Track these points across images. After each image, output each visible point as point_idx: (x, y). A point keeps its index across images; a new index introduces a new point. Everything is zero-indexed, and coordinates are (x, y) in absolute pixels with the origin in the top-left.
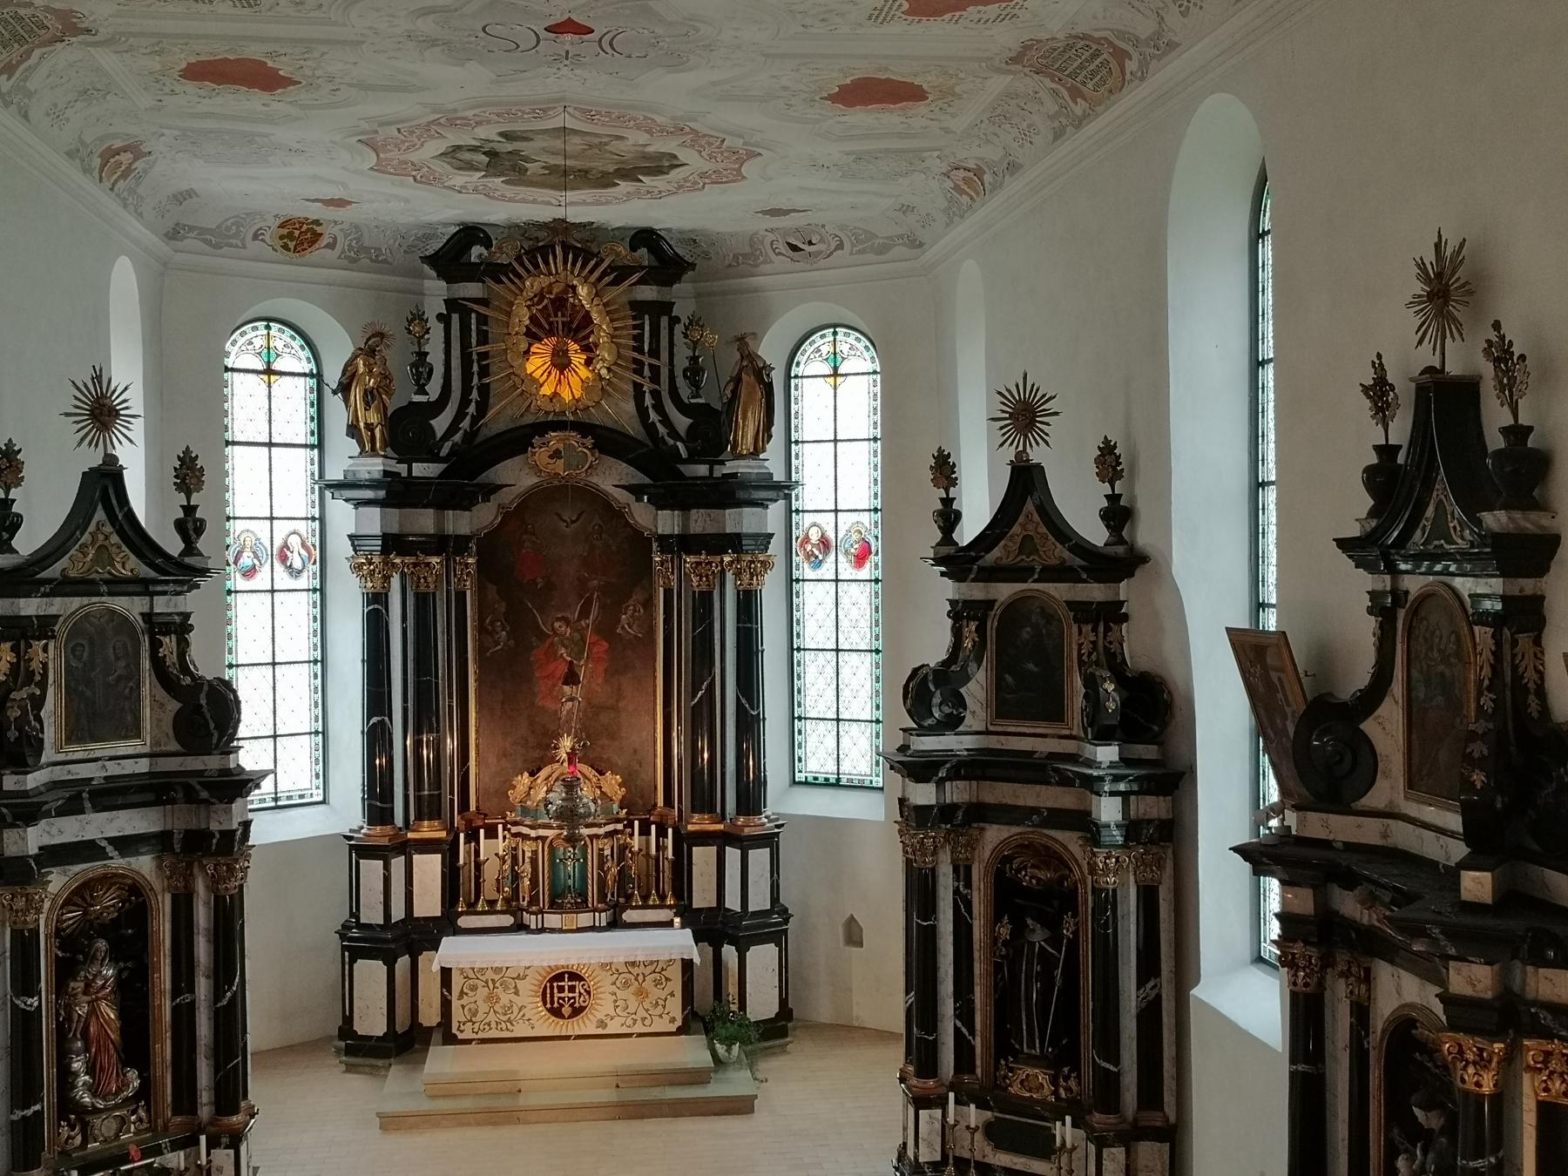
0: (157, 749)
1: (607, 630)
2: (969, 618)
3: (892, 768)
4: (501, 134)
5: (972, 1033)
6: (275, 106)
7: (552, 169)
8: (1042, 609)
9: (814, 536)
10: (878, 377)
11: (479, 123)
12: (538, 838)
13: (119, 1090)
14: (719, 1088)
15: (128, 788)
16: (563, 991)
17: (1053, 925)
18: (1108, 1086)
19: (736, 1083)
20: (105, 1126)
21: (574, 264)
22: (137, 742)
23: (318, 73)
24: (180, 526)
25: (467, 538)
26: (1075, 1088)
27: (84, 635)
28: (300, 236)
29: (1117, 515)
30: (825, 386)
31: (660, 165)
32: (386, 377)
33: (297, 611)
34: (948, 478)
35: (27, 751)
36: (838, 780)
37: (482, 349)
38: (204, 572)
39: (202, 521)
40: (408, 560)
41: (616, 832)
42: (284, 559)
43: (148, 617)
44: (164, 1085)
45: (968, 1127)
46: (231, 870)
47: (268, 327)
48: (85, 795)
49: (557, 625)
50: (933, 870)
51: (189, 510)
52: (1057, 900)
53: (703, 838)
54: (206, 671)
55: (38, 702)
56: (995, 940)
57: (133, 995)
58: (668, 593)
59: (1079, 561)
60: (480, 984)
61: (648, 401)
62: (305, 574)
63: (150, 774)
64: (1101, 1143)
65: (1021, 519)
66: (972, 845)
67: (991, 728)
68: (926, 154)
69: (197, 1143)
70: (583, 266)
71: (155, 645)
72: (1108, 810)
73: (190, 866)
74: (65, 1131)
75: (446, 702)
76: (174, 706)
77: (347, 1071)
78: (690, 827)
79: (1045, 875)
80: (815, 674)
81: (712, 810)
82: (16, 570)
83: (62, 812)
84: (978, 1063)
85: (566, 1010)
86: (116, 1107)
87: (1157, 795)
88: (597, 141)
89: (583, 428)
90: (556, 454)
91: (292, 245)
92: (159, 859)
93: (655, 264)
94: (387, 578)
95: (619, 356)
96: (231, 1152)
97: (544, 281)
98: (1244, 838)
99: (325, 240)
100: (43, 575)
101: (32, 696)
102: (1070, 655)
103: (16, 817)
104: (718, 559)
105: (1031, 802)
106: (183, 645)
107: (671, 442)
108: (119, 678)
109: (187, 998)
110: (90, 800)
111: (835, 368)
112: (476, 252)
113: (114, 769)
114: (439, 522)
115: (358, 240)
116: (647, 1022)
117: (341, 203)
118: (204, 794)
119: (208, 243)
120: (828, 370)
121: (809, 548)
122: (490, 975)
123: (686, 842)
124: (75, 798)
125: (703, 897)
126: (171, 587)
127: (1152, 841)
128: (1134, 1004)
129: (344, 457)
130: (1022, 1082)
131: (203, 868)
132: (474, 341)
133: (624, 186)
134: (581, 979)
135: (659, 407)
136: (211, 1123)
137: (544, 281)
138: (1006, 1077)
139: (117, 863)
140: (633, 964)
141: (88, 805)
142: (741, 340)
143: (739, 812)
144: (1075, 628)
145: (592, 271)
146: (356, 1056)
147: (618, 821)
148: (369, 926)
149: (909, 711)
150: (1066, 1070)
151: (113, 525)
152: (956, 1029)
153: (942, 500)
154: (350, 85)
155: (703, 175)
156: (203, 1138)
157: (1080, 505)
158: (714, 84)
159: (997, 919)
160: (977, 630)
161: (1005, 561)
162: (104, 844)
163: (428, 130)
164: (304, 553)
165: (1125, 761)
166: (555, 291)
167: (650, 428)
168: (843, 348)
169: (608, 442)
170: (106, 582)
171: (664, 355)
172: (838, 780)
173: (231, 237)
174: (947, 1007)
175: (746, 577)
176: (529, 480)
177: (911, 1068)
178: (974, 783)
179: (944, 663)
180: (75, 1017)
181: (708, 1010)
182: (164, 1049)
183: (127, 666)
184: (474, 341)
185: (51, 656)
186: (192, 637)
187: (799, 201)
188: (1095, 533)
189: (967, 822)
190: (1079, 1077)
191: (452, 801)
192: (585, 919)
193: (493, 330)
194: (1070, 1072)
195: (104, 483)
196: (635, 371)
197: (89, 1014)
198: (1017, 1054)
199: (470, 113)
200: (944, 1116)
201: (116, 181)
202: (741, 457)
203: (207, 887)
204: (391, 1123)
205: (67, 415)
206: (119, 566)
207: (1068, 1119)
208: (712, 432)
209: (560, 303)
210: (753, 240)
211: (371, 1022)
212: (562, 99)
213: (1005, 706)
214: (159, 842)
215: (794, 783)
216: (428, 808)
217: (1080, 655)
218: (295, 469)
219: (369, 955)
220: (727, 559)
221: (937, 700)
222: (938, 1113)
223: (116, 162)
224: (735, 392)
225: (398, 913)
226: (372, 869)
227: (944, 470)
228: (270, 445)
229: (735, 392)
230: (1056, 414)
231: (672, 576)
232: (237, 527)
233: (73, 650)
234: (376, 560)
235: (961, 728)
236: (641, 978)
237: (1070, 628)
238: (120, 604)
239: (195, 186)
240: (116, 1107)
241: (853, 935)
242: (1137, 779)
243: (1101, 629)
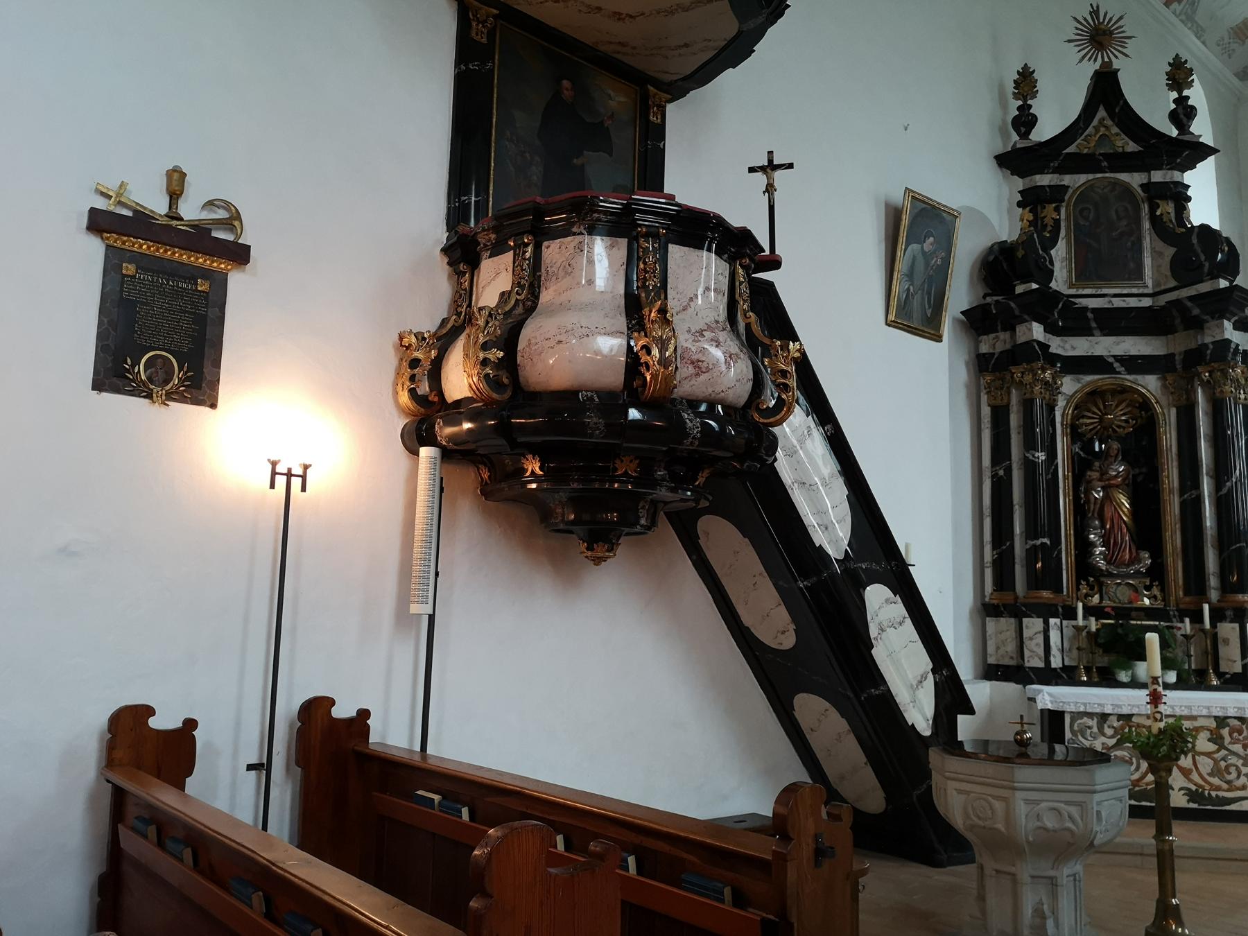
0: (1157, 290)
13: (1132, 562)
24: (1174, 117)
39: (1193, 108)
46: (1225, 374)
51: (1182, 101)
74: (1084, 590)
76: (1170, 251)
92: (1164, 379)
96: (1236, 626)
110: (1095, 319)
113: (1118, 303)
139: (1129, 379)
151: (1113, 120)
162: (1111, 360)
180: (1092, 500)
182: (1173, 538)
185: (1063, 216)
195: (1105, 89)
205: (1069, 41)
233: (1081, 211)
238: (1124, 177)
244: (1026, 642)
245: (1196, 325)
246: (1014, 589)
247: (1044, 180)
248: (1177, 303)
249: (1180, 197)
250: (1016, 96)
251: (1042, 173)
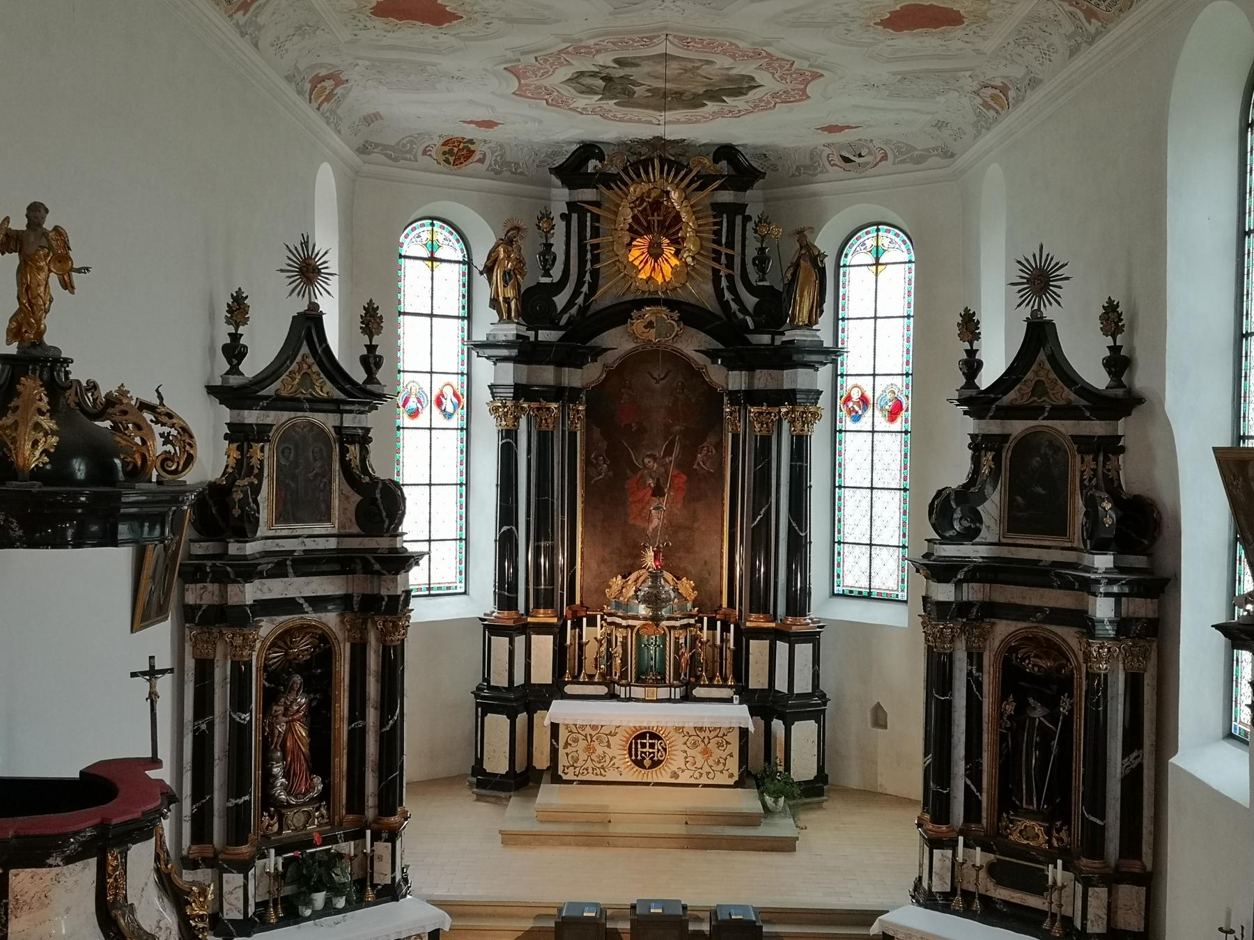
0: (343, 531)
1: (686, 465)
2: (987, 449)
3: (918, 571)
4: (616, 61)
5: (980, 789)
6: (443, 38)
7: (655, 91)
8: (1050, 442)
9: (856, 395)
10: (913, 266)
11: (598, 51)
12: (627, 627)
13: (308, 791)
14: (766, 830)
15: (321, 559)
16: (645, 747)
17: (1051, 704)
18: (1094, 841)
19: (782, 827)
20: (295, 818)
21: (668, 174)
22: (327, 525)
23: (476, 8)
24: (364, 361)
25: (579, 390)
26: (1065, 838)
27: (292, 441)
28: (458, 153)
29: (1118, 363)
30: (868, 273)
31: (740, 86)
32: (520, 261)
33: (449, 444)
34: (973, 333)
35: (247, 526)
36: (870, 593)
37: (595, 241)
38: (381, 397)
39: (381, 357)
40: (534, 405)
41: (689, 625)
42: (439, 403)
43: (339, 429)
44: (340, 791)
45: (974, 866)
46: (395, 626)
47: (432, 225)
48: (289, 563)
49: (646, 460)
50: (951, 656)
51: (371, 348)
52: (1056, 685)
53: (758, 633)
54: (380, 474)
55: (256, 490)
56: (1002, 715)
57: (320, 719)
59: (1083, 402)
61: (724, 283)
62: (455, 416)
63: (336, 550)
64: (1087, 883)
65: (1034, 367)
66: (984, 636)
67: (1003, 540)
68: (960, 74)
69: (364, 837)
70: (675, 176)
71: (344, 451)
72: (1103, 609)
73: (365, 622)
74: (266, 819)
75: (560, 518)
76: (357, 498)
77: (478, 800)
78: (748, 624)
79: (1046, 664)
80: (853, 508)
81: (766, 611)
82: (242, 387)
83: (271, 575)
84: (984, 814)
85: (647, 762)
86: (304, 804)
87: (1145, 597)
88: (690, 65)
89: (672, 304)
90: (650, 325)
91: (451, 159)
92: (342, 615)
94: (517, 419)
95: (702, 247)
97: (645, 187)
98: (1222, 620)
99: (477, 156)
100: (263, 393)
101: (251, 484)
102: (1073, 481)
103: (238, 574)
104: (777, 410)
105: (1035, 602)
106: (364, 453)
107: (741, 316)
108: (316, 475)
109: (360, 723)
110: (292, 566)
111: (877, 259)
112: (592, 165)
113: (311, 544)
114: (558, 376)
115: (502, 156)
116: (711, 776)
117: (489, 124)
118: (377, 567)
119: (389, 157)
120: (870, 259)
121: (851, 404)
122: (588, 731)
123: (744, 635)
124: (282, 565)
125: (757, 680)
126: (355, 407)
127: (1139, 636)
128: (1119, 771)
129: (487, 324)
130: (1021, 832)
131: (374, 623)
132: (588, 235)
133: (711, 106)
134: (659, 738)
135: (733, 289)
136: (374, 822)
137: (645, 187)
138: (1007, 827)
139: (311, 616)
140: (701, 729)
141: (290, 570)
142: (800, 233)
143: (788, 614)
144: (1078, 458)
145: (682, 180)
146: (484, 788)
147: (691, 616)
148: (497, 688)
149: (933, 526)
150: (1058, 823)
152: (966, 786)
153: (967, 351)
154: (500, 19)
155: (775, 95)
156: (368, 832)
157: (1086, 356)
158: (787, 12)
159: (1003, 698)
160: (993, 459)
161: (1019, 402)
162: (302, 601)
163: (558, 58)
164: (455, 400)
165: (1118, 568)
166: (653, 195)
167: (725, 305)
168: (884, 241)
169: (691, 315)
170: (308, 400)
171: (738, 247)
172: (870, 593)
173: (408, 152)
175: (799, 425)
176: (628, 346)
177: (927, 816)
178: (988, 586)
179: (964, 486)
181: (759, 769)
182: (341, 762)
183: (322, 466)
184: (588, 235)
186: (371, 446)
187: (852, 119)
188: (1098, 379)
189: (980, 619)
190: (1069, 830)
191: (562, 595)
192: (663, 692)
193: (603, 226)
194: (1062, 826)
195: (308, 325)
196: (714, 259)
197: (286, 732)
198: (1017, 810)
199: (591, 42)
200: (954, 855)
201: (320, 105)
202: (799, 327)
203: (377, 640)
204: (509, 839)
205: (282, 271)
206: (318, 390)
207: (1060, 862)
208: (775, 308)
209: (656, 205)
210: (813, 154)
211: (497, 763)
212: (665, 28)
213: (1015, 522)
214: (344, 602)
215: (834, 595)
216: (544, 599)
217: (1082, 481)
218: (450, 335)
220: (784, 410)
221: (957, 515)
222: (949, 853)
223: (322, 87)
224: (794, 275)
225: (519, 679)
226: (500, 643)
227: (969, 326)
228: (432, 316)
229: (794, 275)
230: (1067, 278)
231: (739, 425)
232: (405, 378)
233: (283, 452)
234: (509, 404)
235: (977, 540)
236: (706, 741)
237: (1074, 457)
238: (318, 418)
239: (382, 110)
240: (304, 804)
241: (879, 718)
242: (1128, 583)
243: (1101, 459)
244: (226, 896)
246: (211, 842)
247: (251, 417)
250: (228, 323)
251: (250, 409)
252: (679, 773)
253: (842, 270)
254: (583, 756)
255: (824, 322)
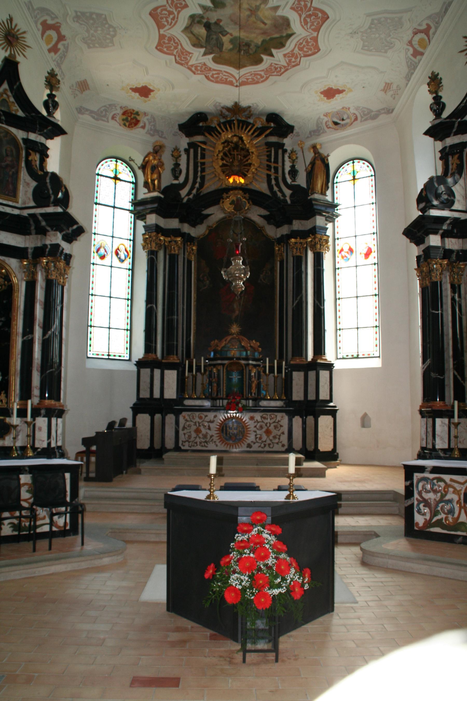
0: (24, 206)
9: (346, 249)
24: (46, 104)
28: (131, 119)
33: (122, 277)
36: (358, 355)
37: (203, 161)
42: (117, 254)
47: (117, 162)
53: (298, 368)
58: (282, 263)
60: (192, 423)
61: (273, 182)
71: (28, 154)
75: (181, 306)
91: (127, 124)
93: (275, 126)
96: (46, 419)
99: (141, 124)
108: (7, 166)
109: (30, 336)
111: (354, 177)
116: (271, 446)
119: (93, 118)
121: (343, 253)
132: (199, 157)
145: (249, 131)
151: (12, 92)
152: (455, 376)
160: (458, 158)
164: (126, 254)
167: (274, 193)
171: (280, 164)
174: (450, 363)
184: (199, 157)
193: (207, 154)
196: (267, 170)
215: (337, 359)
219: (143, 412)
220: (310, 240)
222: (446, 420)
226: (146, 372)
235: (453, 208)
236: (268, 425)
238: (13, 130)
245: (42, 232)
248: (33, 216)
249: (43, 152)
252: (252, 444)
253: (335, 185)
254: (194, 435)
255: (329, 193)
